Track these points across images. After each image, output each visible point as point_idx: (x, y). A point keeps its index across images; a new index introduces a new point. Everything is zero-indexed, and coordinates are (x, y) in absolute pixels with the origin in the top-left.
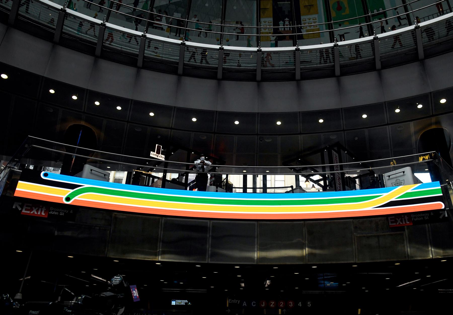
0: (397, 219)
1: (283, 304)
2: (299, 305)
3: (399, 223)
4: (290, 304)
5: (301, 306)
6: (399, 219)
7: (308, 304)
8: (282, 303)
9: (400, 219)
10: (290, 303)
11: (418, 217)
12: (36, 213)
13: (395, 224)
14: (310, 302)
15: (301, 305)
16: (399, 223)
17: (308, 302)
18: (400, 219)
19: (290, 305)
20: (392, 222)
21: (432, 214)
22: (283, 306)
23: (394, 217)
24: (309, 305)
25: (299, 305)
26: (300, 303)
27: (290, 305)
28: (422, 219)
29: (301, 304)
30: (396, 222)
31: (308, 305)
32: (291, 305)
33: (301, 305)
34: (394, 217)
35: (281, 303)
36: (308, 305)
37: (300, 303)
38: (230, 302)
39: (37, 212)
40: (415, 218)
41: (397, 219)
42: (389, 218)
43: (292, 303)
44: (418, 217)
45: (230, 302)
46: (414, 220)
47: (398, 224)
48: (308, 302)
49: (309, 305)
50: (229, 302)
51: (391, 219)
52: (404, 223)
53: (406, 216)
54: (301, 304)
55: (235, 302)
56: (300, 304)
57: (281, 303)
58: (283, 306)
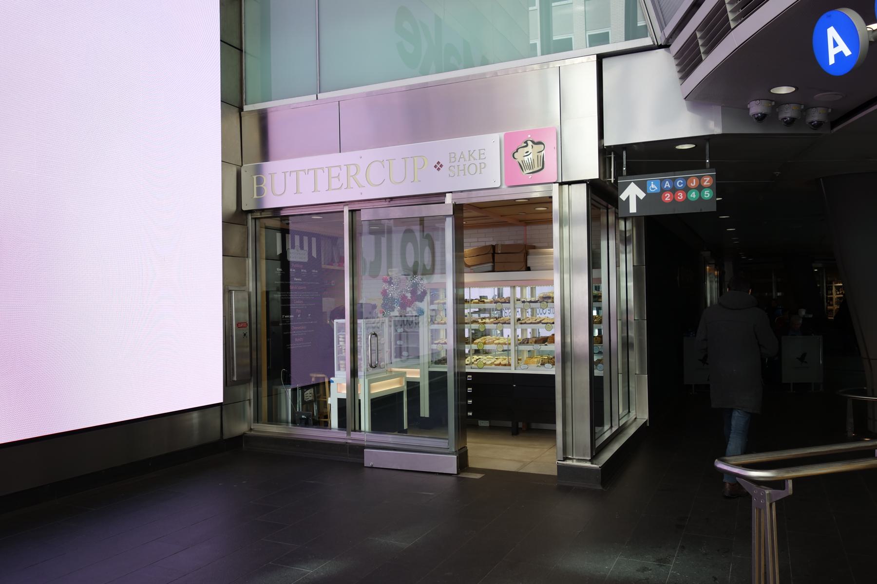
1: (669, 196)
2: (691, 196)
4: (679, 196)
5: (694, 197)
7: (705, 194)
8: (668, 196)
10: (679, 194)
14: (708, 191)
15: (694, 196)
17: (706, 192)
19: (679, 198)
22: (669, 199)
24: (707, 195)
25: (691, 196)
26: (694, 193)
27: (679, 198)
29: (694, 194)
31: (705, 196)
32: (680, 197)
33: (694, 196)
35: (666, 195)
36: (705, 196)
37: (694, 193)
43: (682, 194)
48: (706, 192)
49: (707, 195)
57: (666, 195)
58: (669, 199)
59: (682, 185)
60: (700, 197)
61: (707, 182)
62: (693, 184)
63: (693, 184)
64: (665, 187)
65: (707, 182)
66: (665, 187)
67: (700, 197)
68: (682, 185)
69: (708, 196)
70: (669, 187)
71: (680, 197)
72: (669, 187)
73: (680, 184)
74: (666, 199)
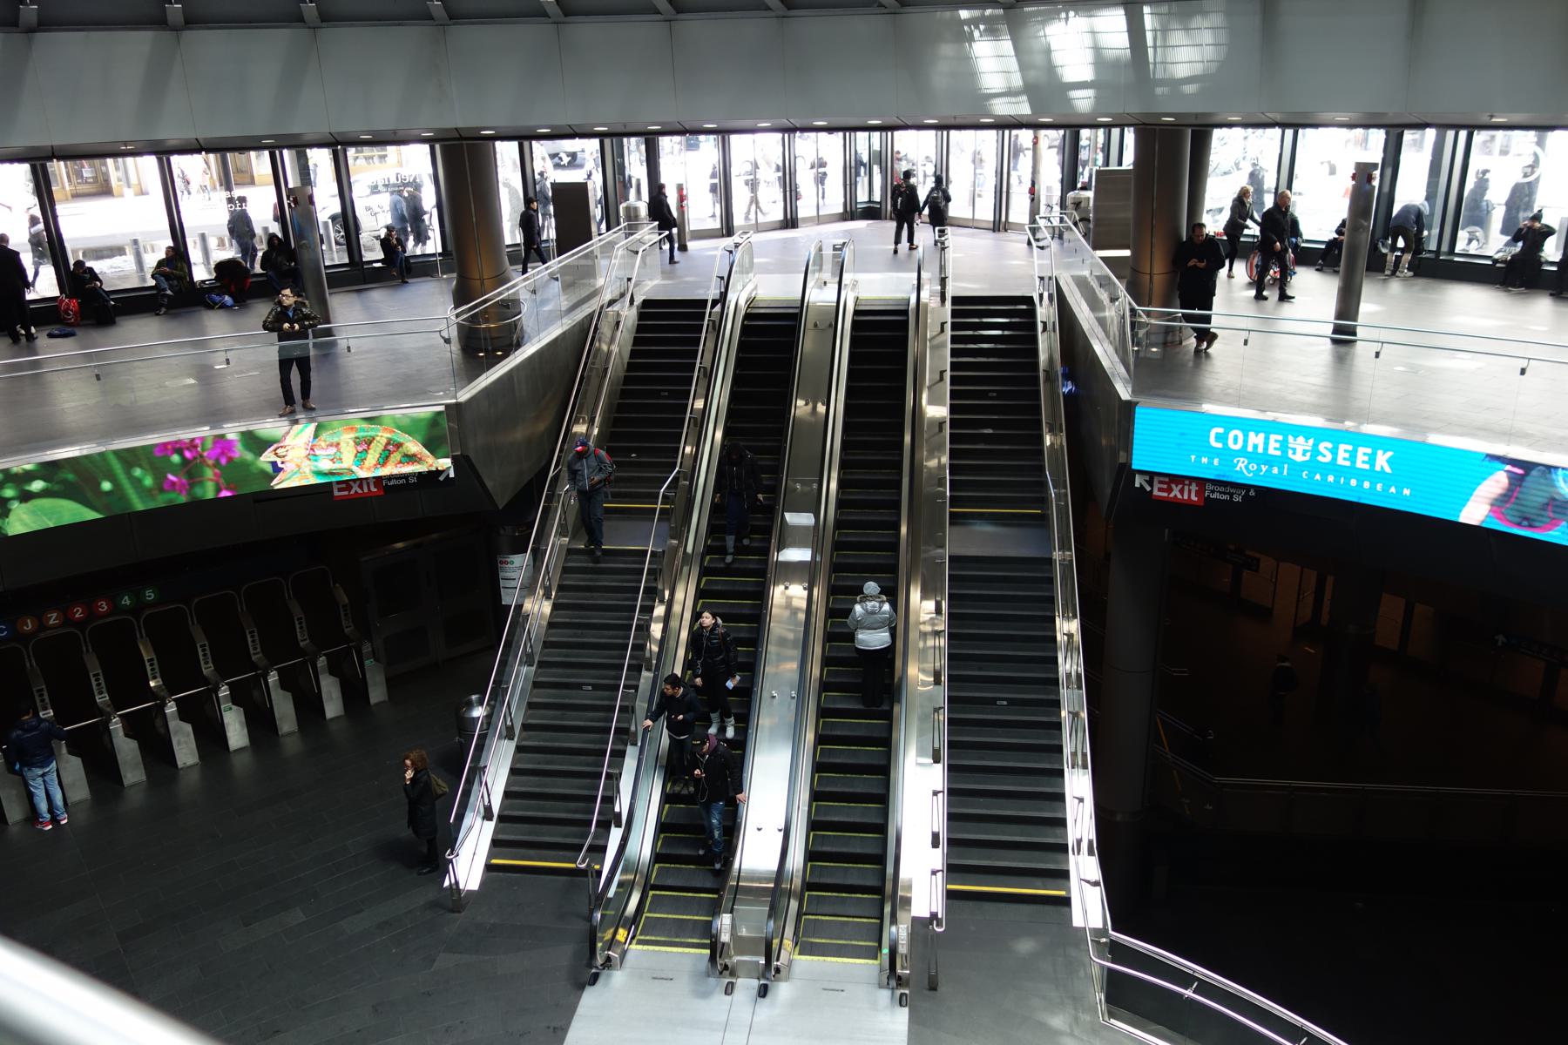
0: (1173, 486)
3: (1176, 496)
6: (1177, 486)
9: (1180, 486)
11: (1219, 491)
12: (360, 491)
13: (1165, 494)
16: (1176, 496)
18: (1180, 486)
20: (1160, 490)
21: (1252, 493)
23: (1167, 480)
28: (1225, 497)
30: (1170, 490)
34: (1167, 480)
39: (362, 488)
40: (1213, 492)
41: (1173, 486)
42: (1156, 480)
44: (1221, 493)
46: (1209, 496)
47: (1172, 495)
51: (1160, 482)
52: (1186, 497)
53: (1194, 485)
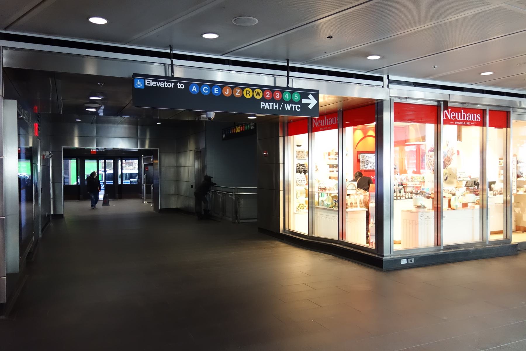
2: (285, 97)
15: (287, 97)
19: (276, 96)
24: (296, 98)
25: (285, 97)
27: (276, 96)
31: (295, 98)
32: (278, 96)
33: (287, 97)
38: (148, 84)
45: (148, 84)
49: (296, 98)
50: (146, 85)
54: (288, 96)
55: (166, 86)
56: (286, 96)
59: (207, 91)
60: (292, 99)
61: (238, 91)
62: (227, 93)
63: (227, 93)
64: (193, 91)
65: (238, 91)
66: (193, 91)
67: (292, 99)
68: (207, 91)
69: (297, 99)
70: (196, 91)
71: (278, 96)
72: (196, 91)
73: (206, 90)
74: (267, 96)
